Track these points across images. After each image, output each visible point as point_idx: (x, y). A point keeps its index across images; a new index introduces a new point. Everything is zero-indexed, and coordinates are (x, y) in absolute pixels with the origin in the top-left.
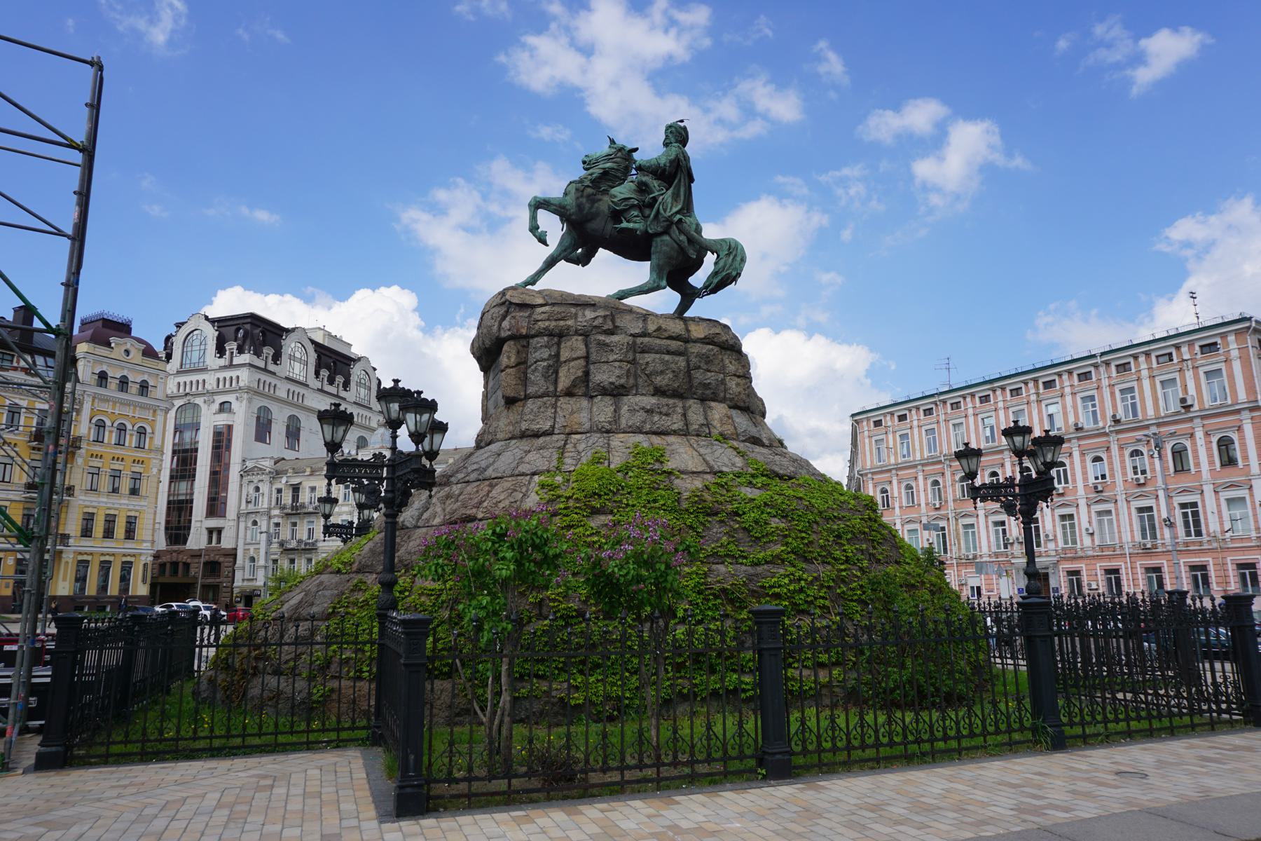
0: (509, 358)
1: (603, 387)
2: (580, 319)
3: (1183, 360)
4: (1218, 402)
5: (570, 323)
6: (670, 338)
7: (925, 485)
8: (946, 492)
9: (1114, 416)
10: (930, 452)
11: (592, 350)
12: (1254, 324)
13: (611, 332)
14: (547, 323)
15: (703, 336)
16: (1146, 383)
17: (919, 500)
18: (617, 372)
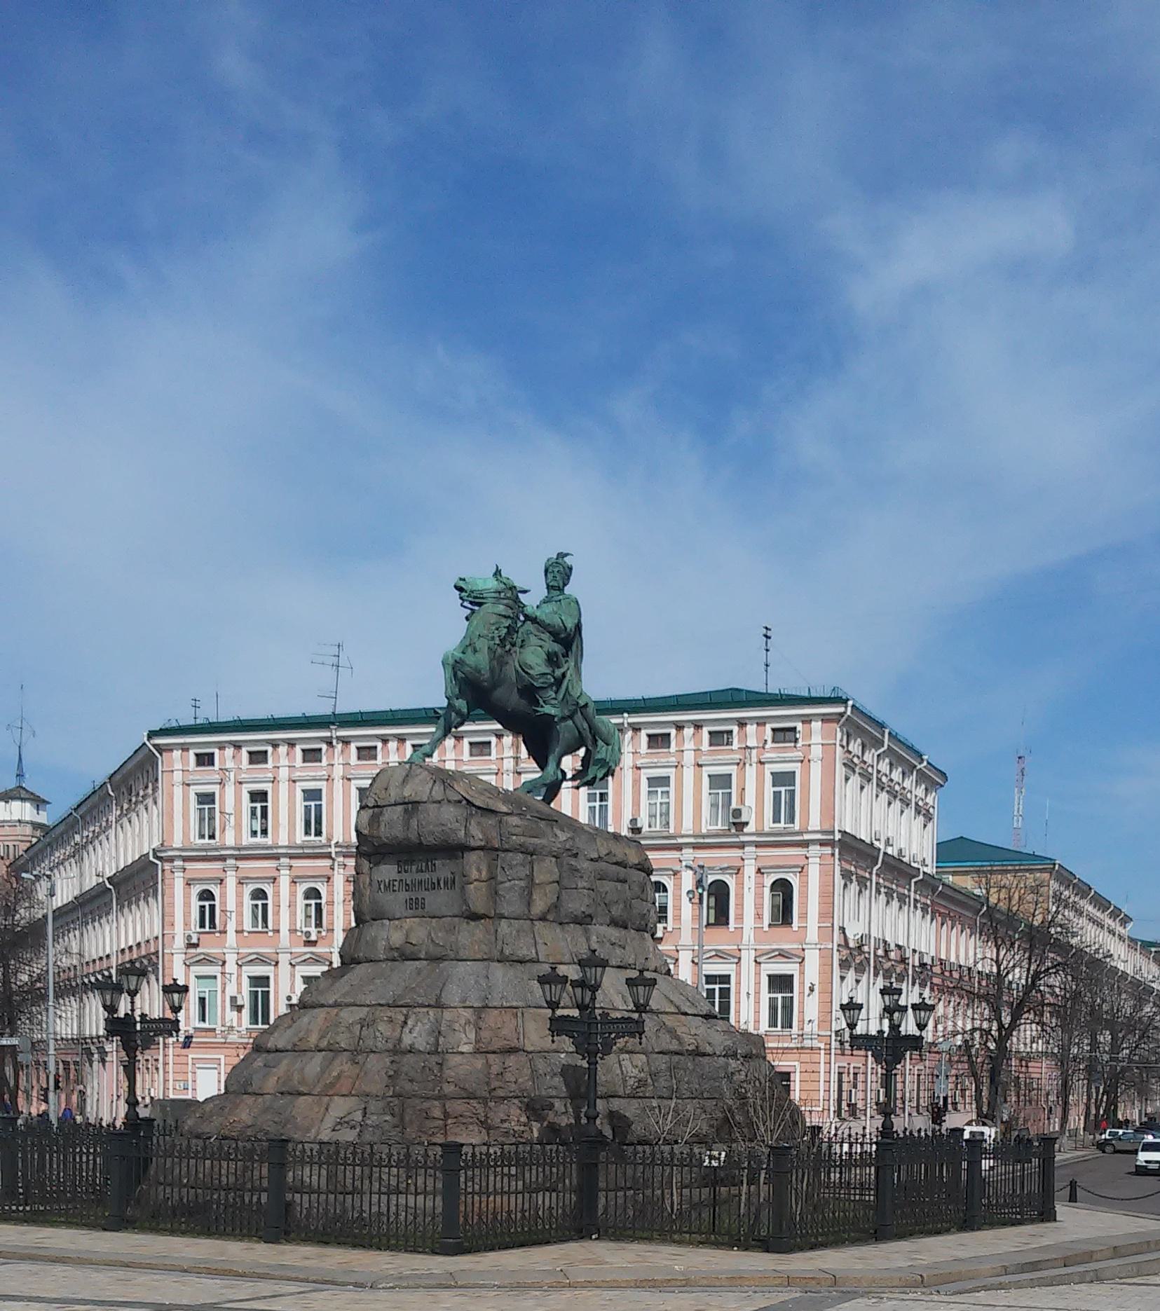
0: (479, 870)
1: (576, 916)
2: (553, 840)
3: (747, 747)
4: (782, 825)
5: (543, 841)
6: (616, 863)
7: (293, 894)
8: (331, 913)
9: (634, 821)
10: (307, 833)
11: (564, 875)
12: (849, 713)
13: (576, 855)
14: (522, 839)
15: (637, 862)
16: (689, 773)
17: (277, 922)
18: (586, 901)
